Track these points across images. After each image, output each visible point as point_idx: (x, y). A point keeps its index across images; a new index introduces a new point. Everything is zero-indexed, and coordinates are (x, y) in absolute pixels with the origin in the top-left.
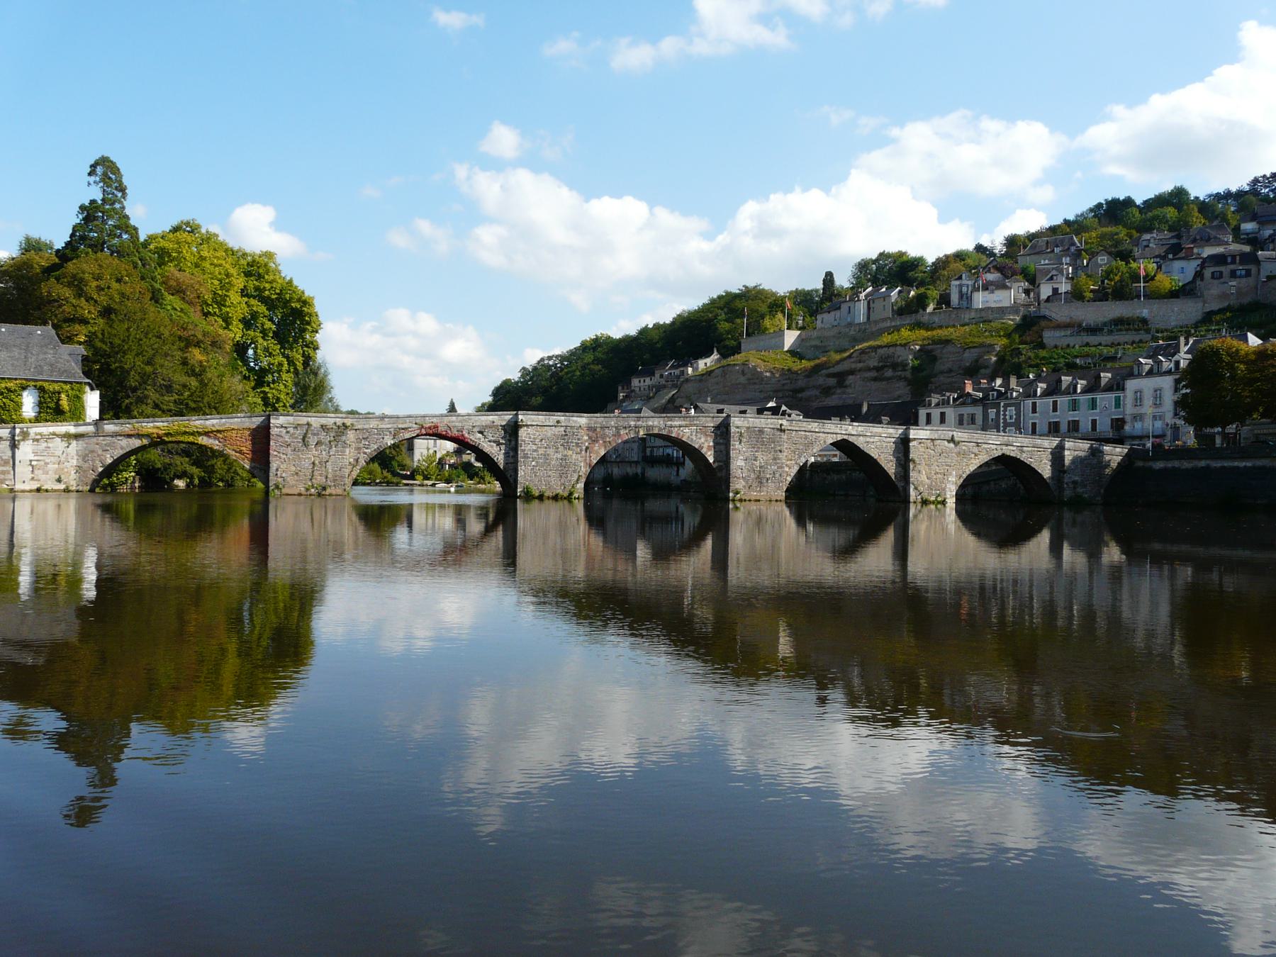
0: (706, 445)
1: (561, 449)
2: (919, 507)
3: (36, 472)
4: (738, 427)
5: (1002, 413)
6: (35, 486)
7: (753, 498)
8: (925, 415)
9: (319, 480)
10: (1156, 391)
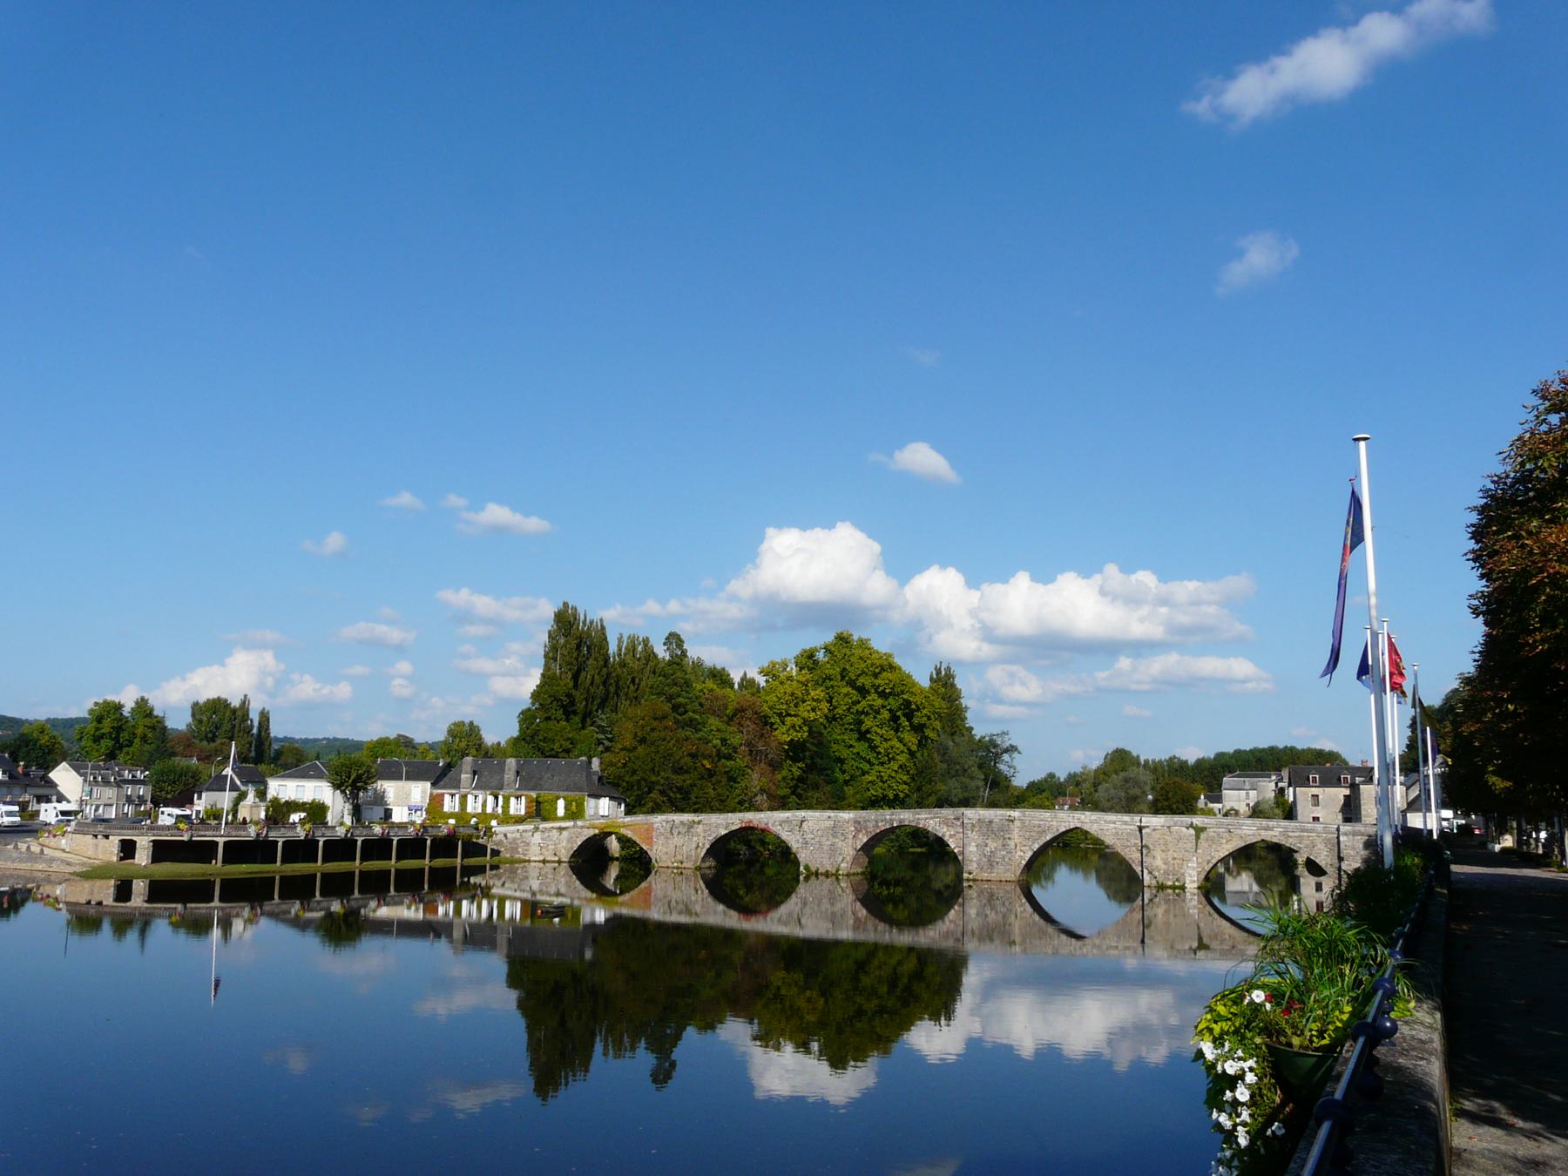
0: (948, 833)
1: (831, 838)
2: (1154, 892)
3: (543, 850)
4: (970, 819)
6: (541, 858)
7: (984, 879)
9: (679, 857)
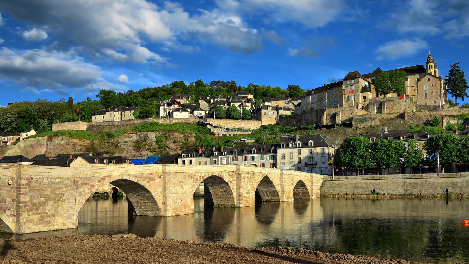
5: (220, 161)
8: (189, 161)
10: (291, 153)
